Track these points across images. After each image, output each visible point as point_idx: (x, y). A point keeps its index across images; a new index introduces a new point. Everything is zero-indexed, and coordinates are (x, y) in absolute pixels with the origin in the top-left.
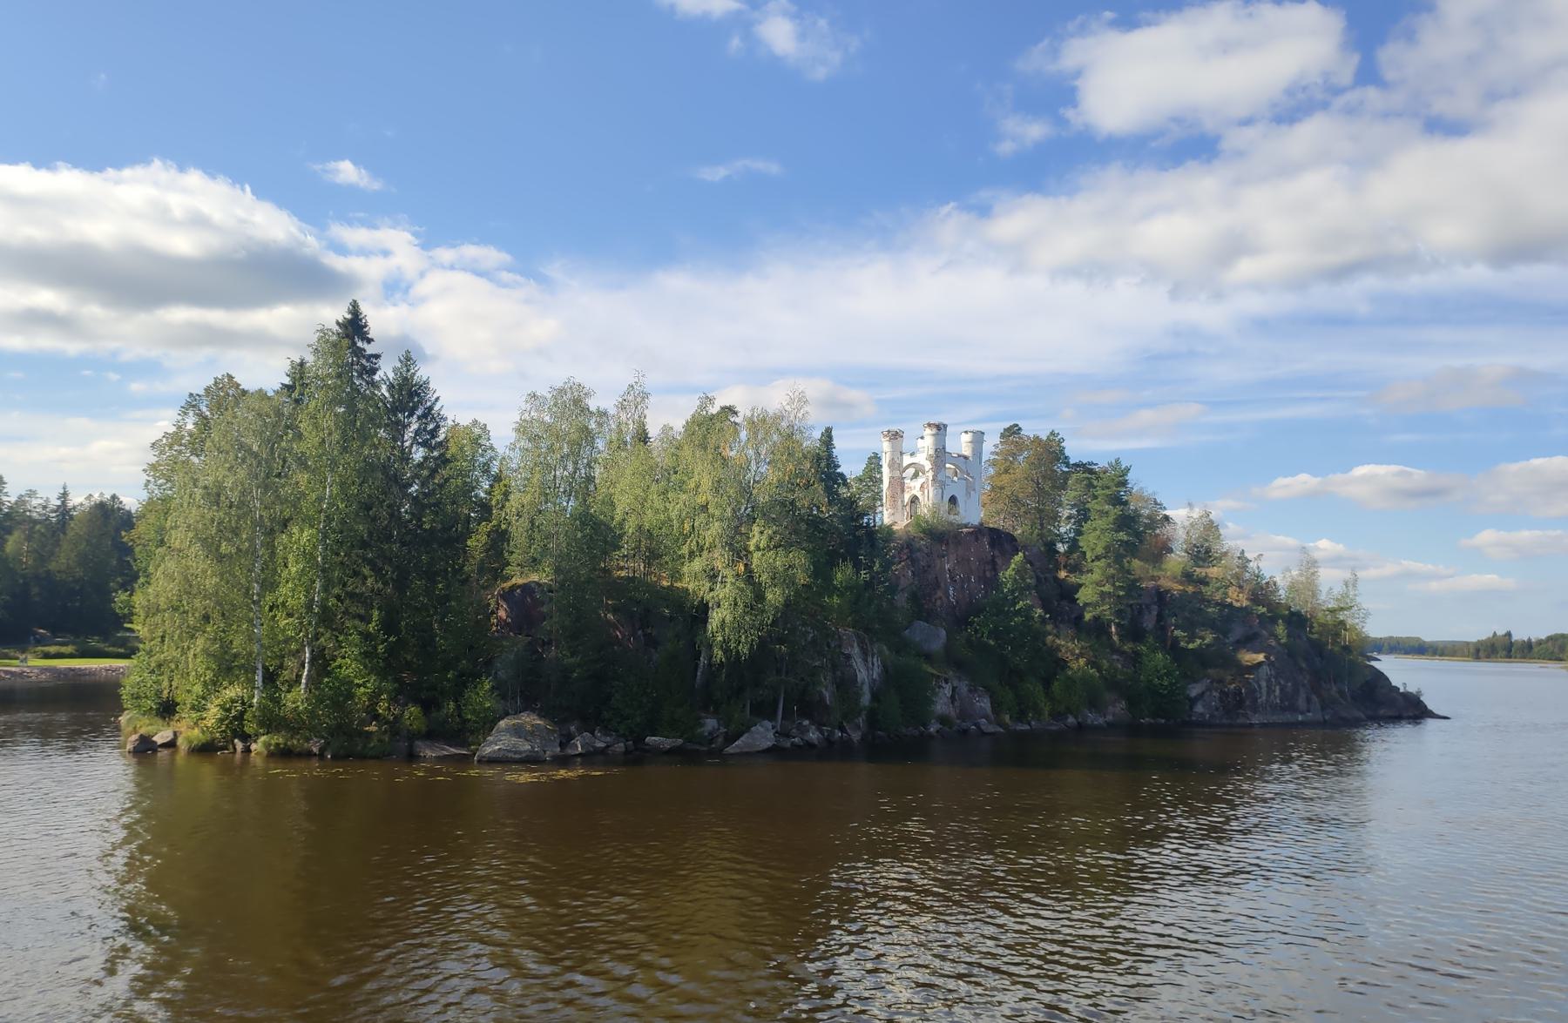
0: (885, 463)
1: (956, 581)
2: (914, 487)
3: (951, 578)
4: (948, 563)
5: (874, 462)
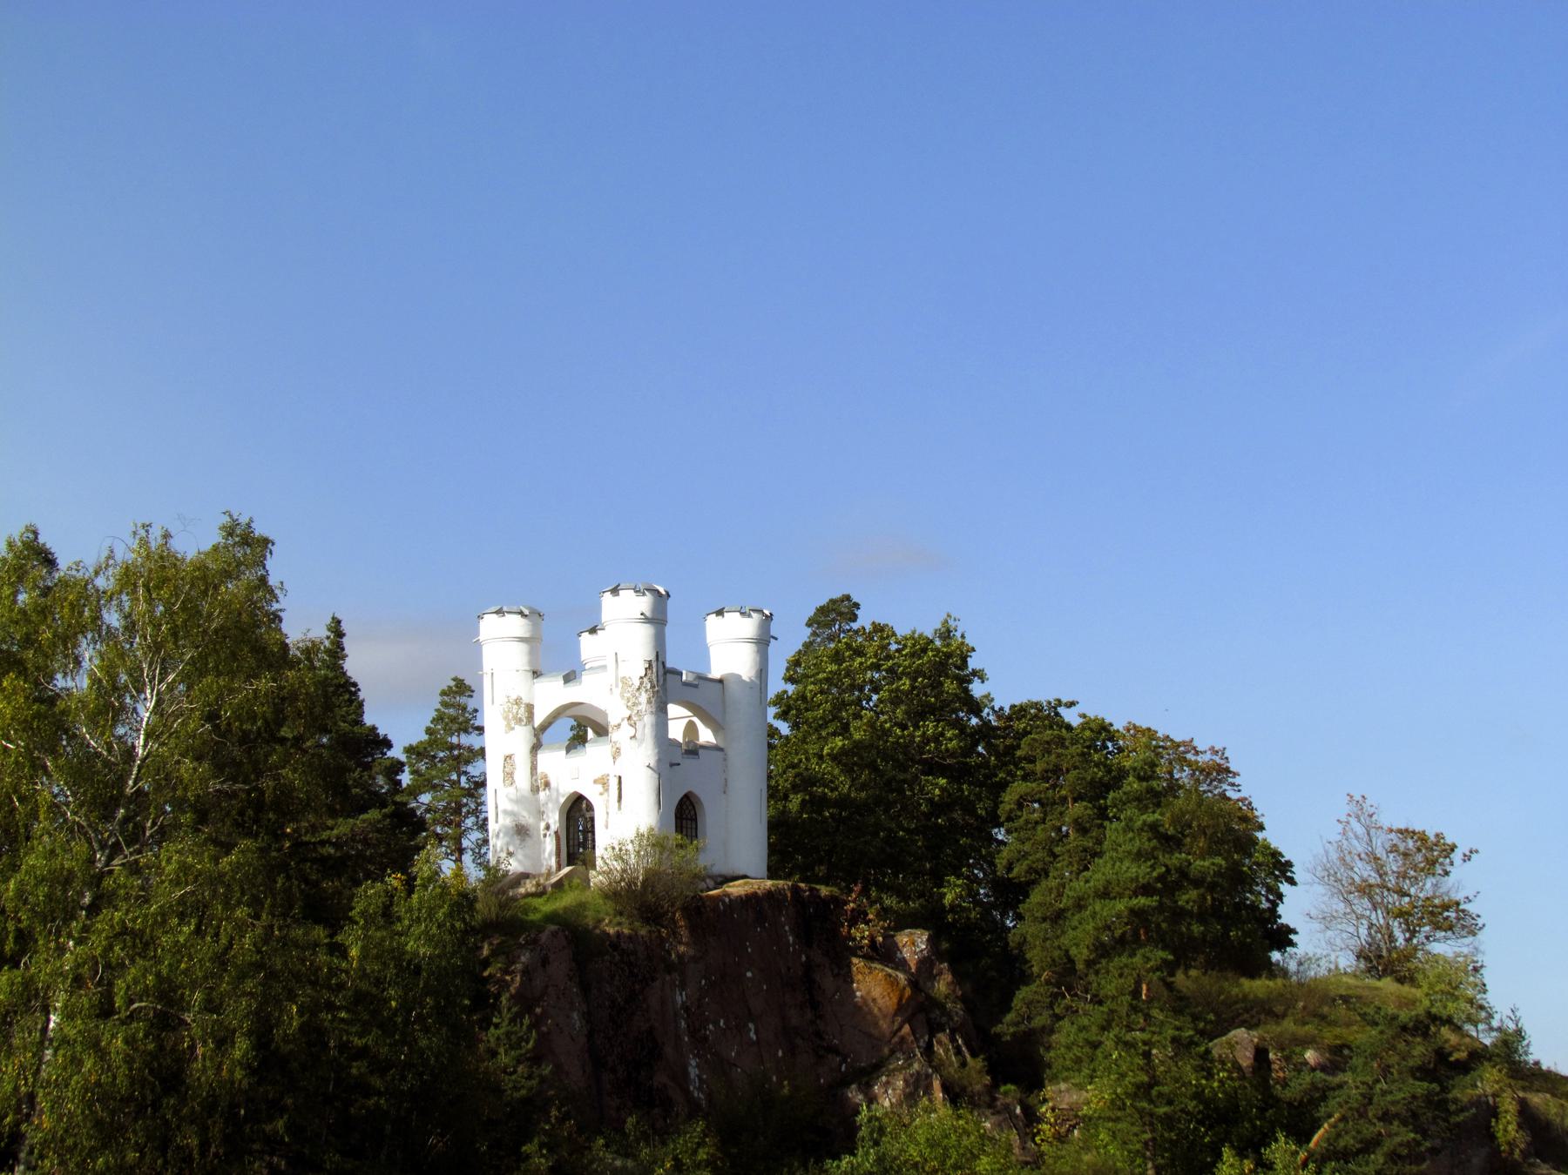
1: (706, 1038)
3: (693, 1032)
4: (683, 987)
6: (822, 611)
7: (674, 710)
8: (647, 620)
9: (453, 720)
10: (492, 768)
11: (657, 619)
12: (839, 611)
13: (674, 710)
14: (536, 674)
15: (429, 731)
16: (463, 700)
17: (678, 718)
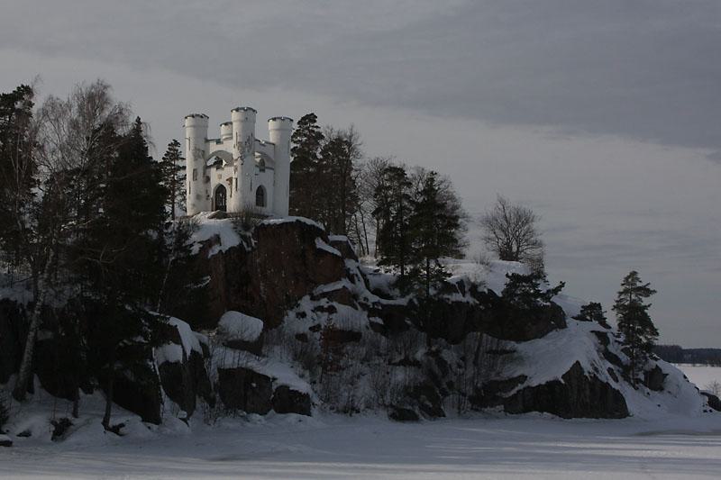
0: (187, 153)
2: (217, 177)
5: (174, 152)
6: (303, 118)
9: (173, 154)
10: (189, 172)
12: (311, 118)
15: (163, 158)
16: (177, 148)
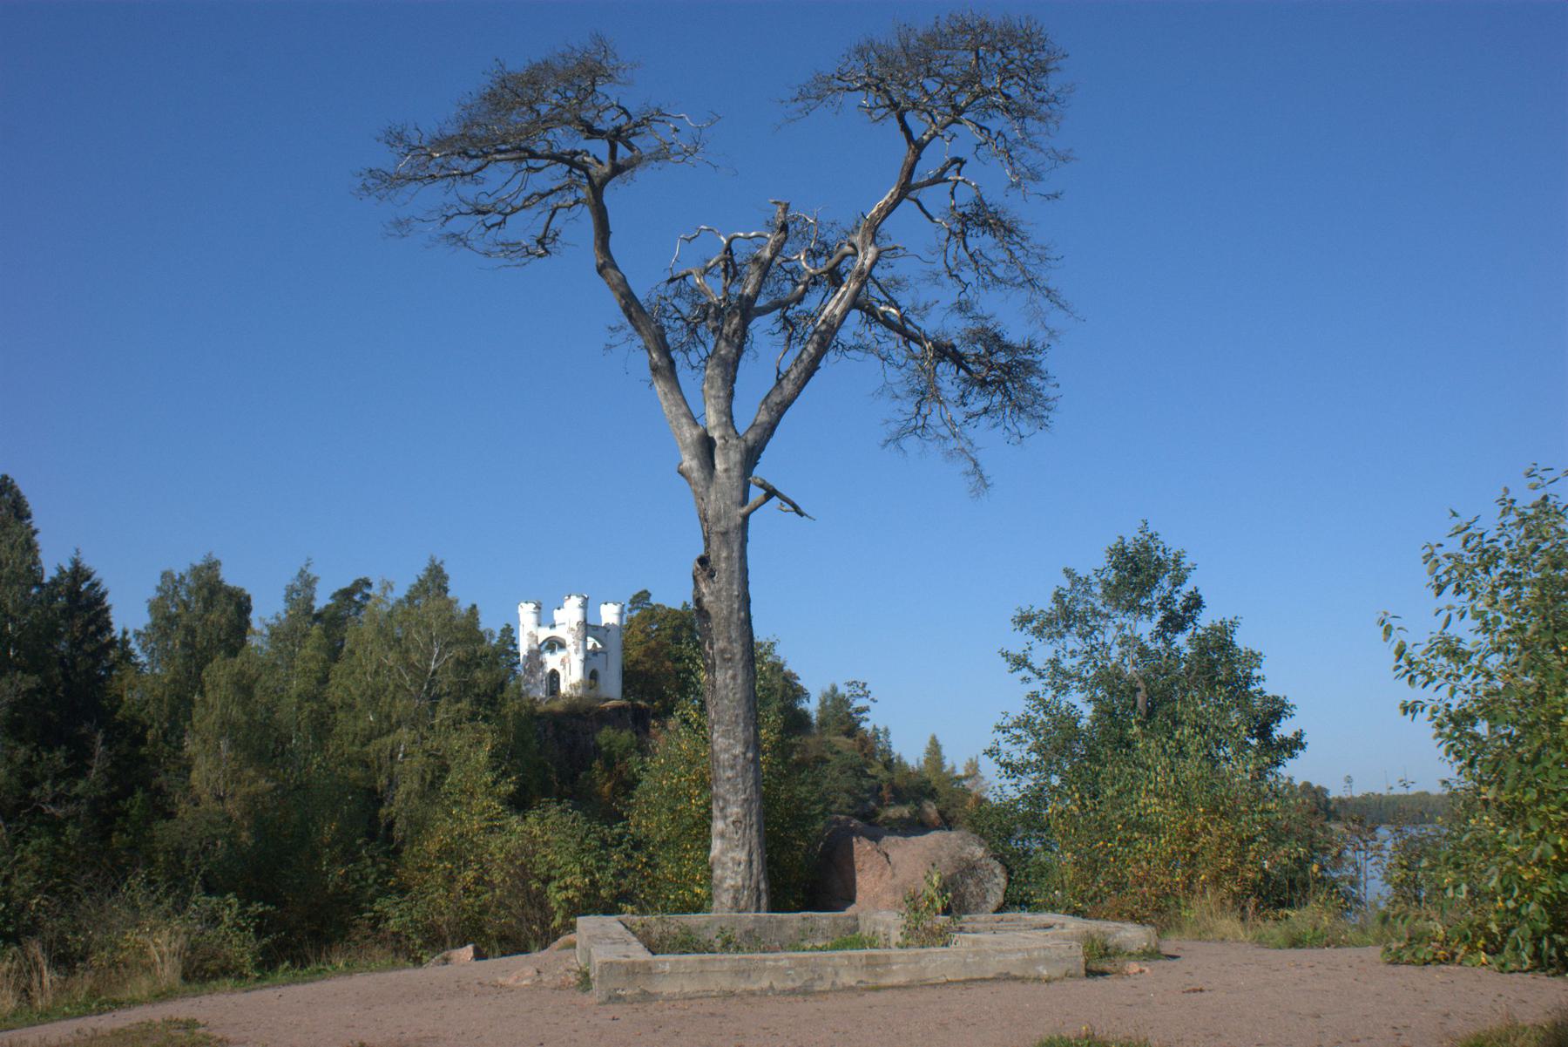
6: (636, 597)
7: (589, 639)
8: (580, 607)
11: (585, 606)
13: (589, 639)
14: (539, 625)
17: (591, 641)
